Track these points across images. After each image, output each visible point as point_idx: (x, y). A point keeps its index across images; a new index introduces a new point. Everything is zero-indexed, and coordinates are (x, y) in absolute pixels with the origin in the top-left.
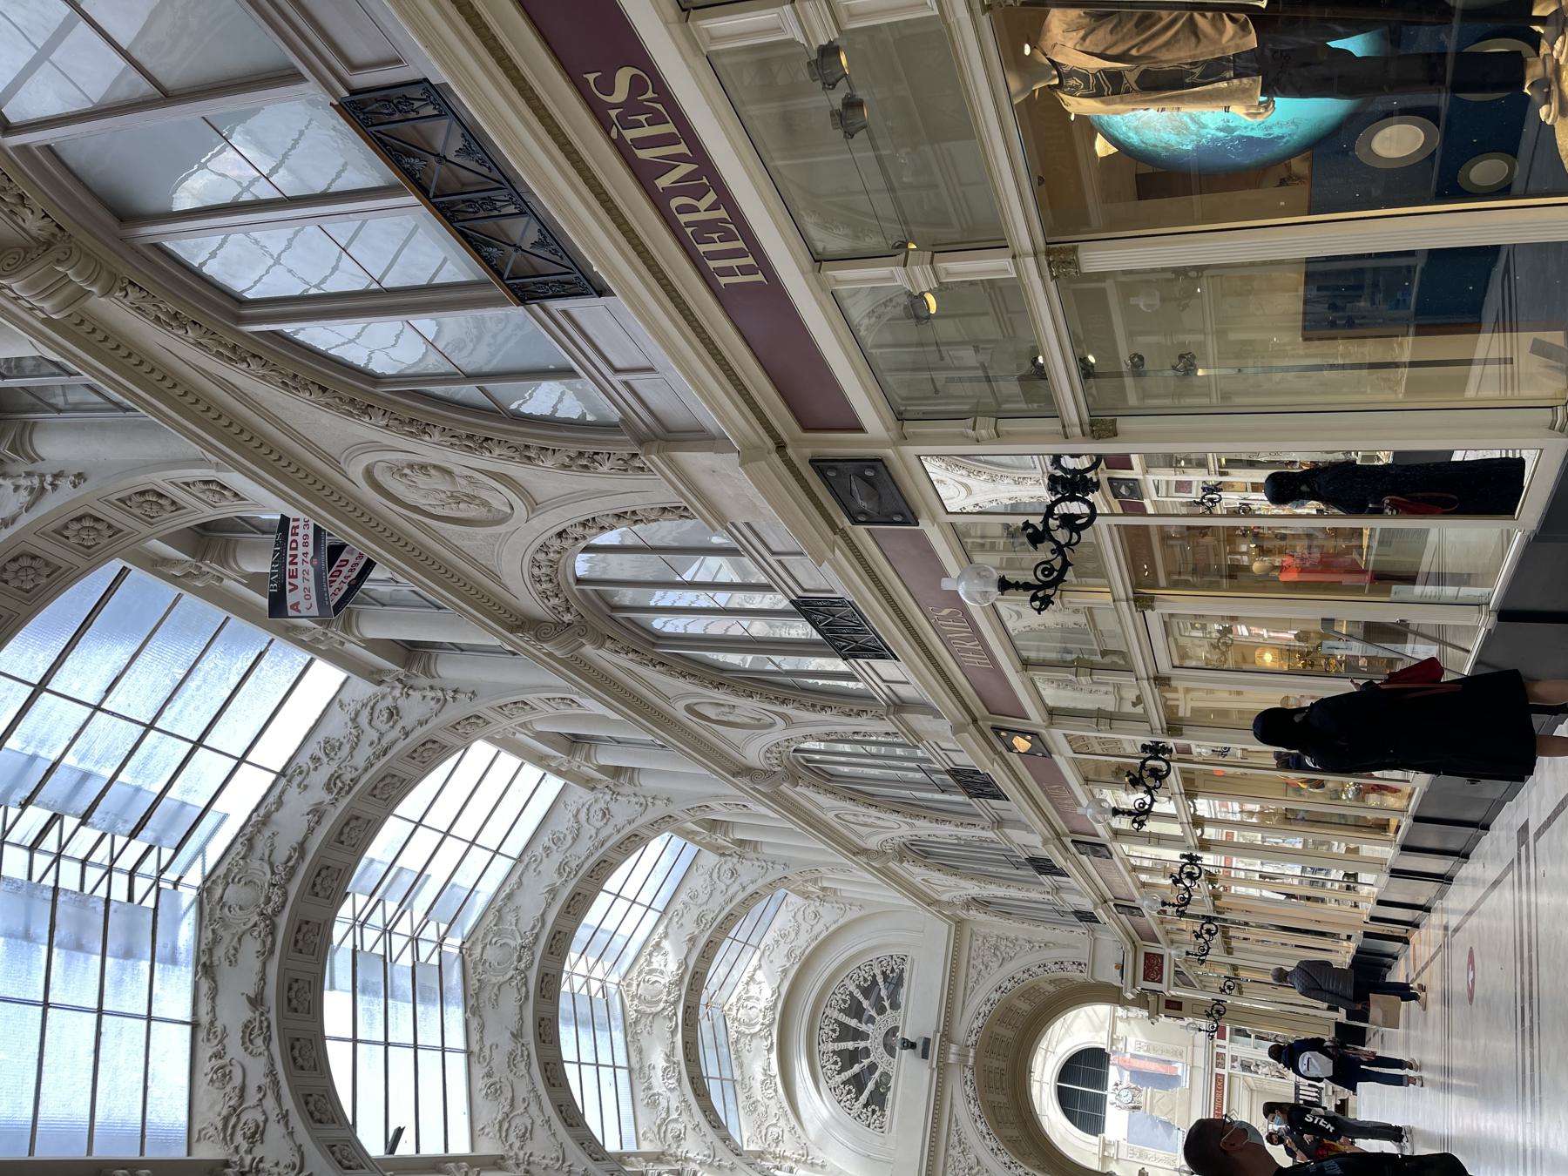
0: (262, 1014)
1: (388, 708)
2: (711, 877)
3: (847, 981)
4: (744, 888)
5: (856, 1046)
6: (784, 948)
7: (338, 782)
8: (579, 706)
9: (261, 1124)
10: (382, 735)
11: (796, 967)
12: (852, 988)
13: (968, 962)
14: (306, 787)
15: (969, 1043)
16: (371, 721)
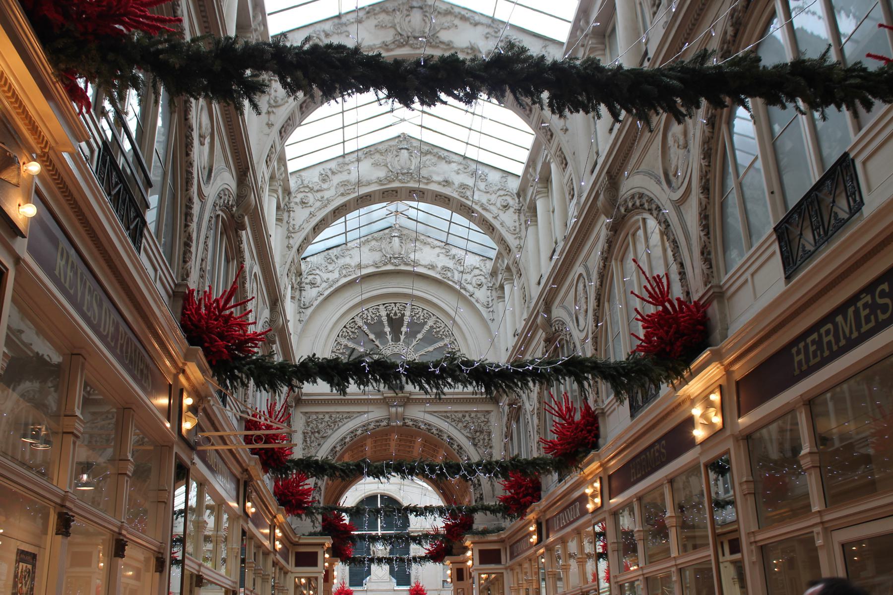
2: (499, 190)
3: (433, 319)
4: (495, 218)
5: (388, 333)
6: (450, 264)
8: (654, 14)
12: (430, 323)
13: (466, 412)
15: (406, 421)
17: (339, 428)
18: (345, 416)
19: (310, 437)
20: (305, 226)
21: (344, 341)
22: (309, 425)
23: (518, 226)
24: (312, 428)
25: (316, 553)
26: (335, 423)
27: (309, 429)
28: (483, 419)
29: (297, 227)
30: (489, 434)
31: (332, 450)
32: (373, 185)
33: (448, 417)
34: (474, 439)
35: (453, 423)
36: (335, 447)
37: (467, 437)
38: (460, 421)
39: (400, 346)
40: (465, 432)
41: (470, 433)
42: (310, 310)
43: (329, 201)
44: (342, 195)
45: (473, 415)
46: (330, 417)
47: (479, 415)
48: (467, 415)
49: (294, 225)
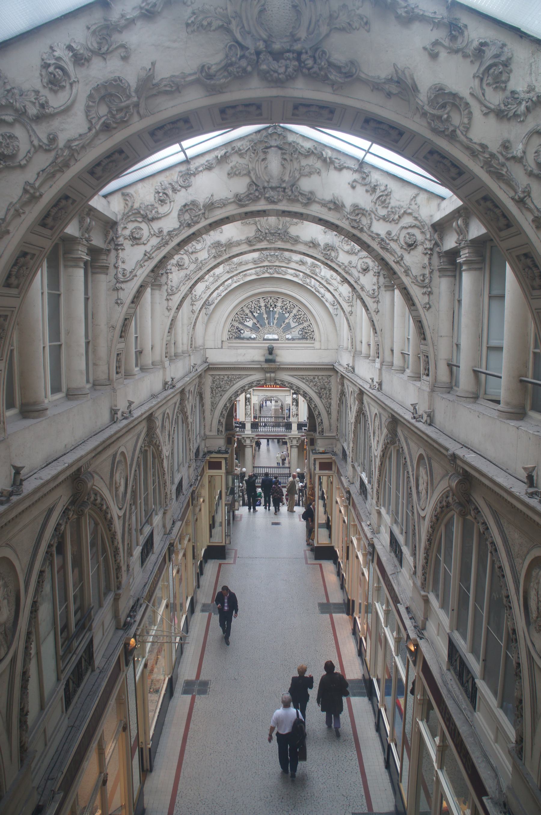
0: (204, 214)
1: (415, 242)
3: (297, 308)
4: (336, 290)
7: (360, 216)
9: (142, 241)
10: (396, 241)
11: (300, 282)
14: (353, 187)
15: (277, 381)
16: (406, 228)
17: (234, 385)
18: (237, 377)
19: (215, 390)
20: (203, 296)
21: (236, 324)
22: (214, 383)
23: (351, 297)
24: (216, 385)
25: (221, 462)
26: (231, 381)
27: (215, 385)
28: (326, 380)
29: (198, 297)
30: (330, 390)
31: (229, 399)
32: (249, 264)
33: (304, 379)
34: (320, 393)
35: (307, 383)
36: (231, 397)
37: (316, 392)
38: (311, 381)
39: (274, 328)
40: (314, 389)
41: (318, 389)
42: (212, 307)
43: (219, 277)
44: (228, 272)
45: (320, 377)
46: (228, 377)
47: (324, 378)
48: (316, 377)
49: (196, 295)
